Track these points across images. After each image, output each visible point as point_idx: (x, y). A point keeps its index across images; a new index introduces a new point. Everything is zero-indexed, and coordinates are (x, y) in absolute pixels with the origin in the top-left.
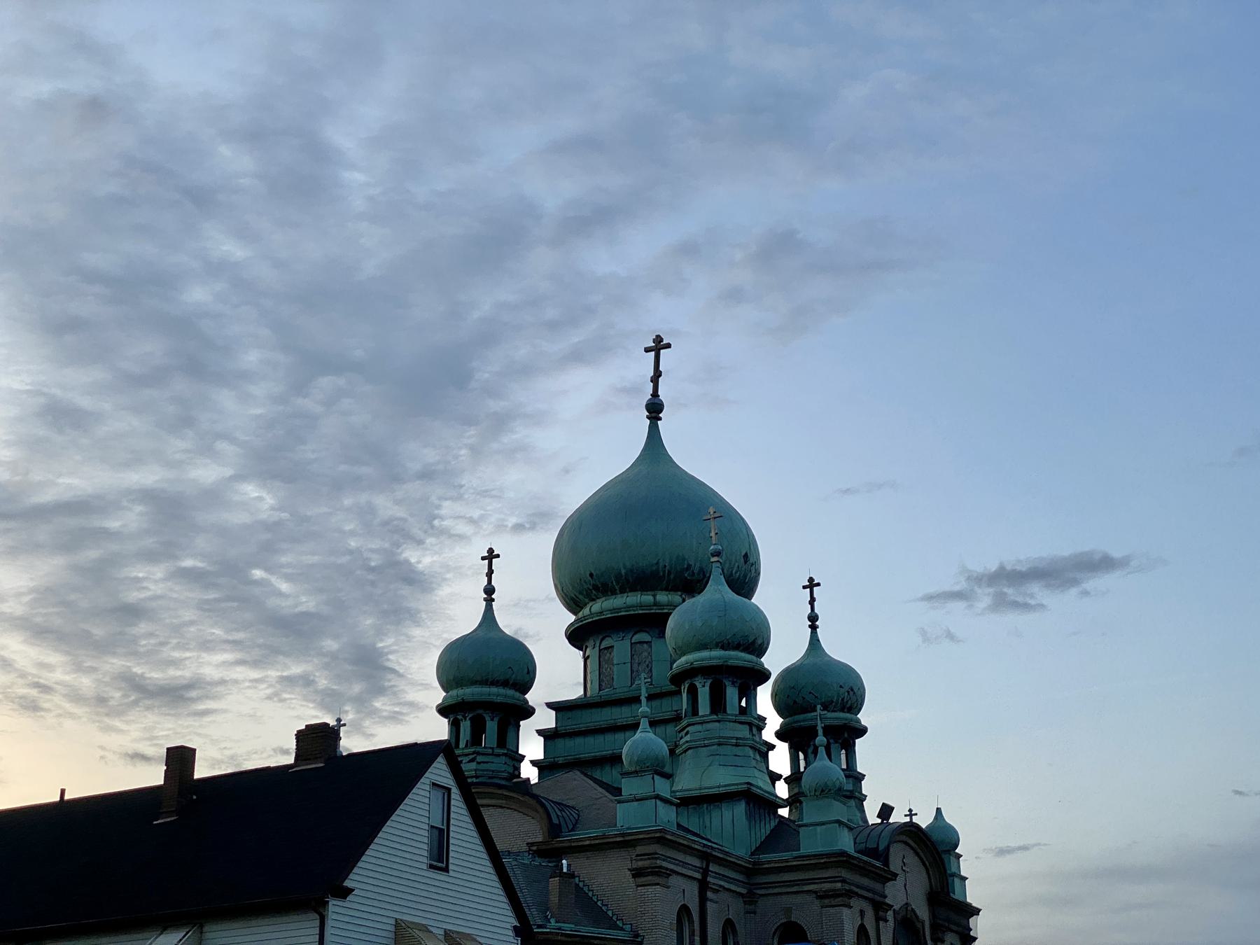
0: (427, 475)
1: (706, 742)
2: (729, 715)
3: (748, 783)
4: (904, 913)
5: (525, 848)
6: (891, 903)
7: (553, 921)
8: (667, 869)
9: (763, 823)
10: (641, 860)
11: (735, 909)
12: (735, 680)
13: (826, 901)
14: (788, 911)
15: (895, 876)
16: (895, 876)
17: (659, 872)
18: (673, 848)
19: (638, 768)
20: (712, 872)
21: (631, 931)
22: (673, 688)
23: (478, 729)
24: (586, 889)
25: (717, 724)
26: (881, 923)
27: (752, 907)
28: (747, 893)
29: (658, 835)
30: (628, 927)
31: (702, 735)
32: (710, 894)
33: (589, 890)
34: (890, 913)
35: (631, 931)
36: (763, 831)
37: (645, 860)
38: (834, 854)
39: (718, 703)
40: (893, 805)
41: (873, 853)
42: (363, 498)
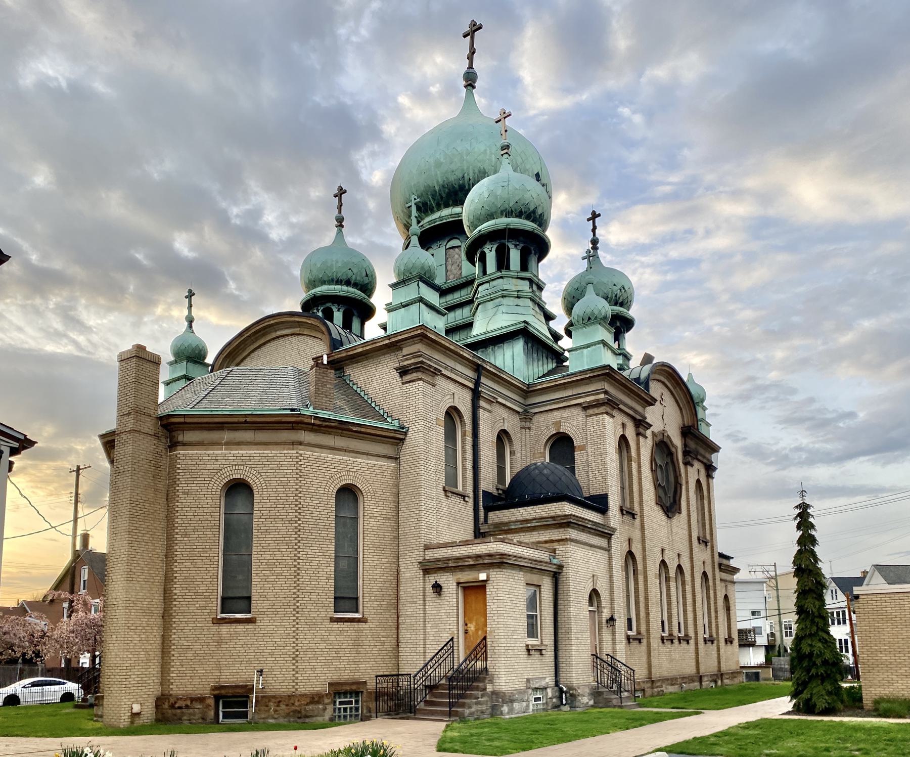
1: (492, 296)
3: (525, 322)
6: (651, 423)
7: (311, 409)
10: (407, 359)
11: (511, 423)
13: (590, 411)
17: (419, 368)
18: (445, 354)
25: (501, 280)
26: (641, 438)
30: (396, 423)
31: (490, 291)
32: (482, 403)
33: (365, 395)
34: (649, 433)
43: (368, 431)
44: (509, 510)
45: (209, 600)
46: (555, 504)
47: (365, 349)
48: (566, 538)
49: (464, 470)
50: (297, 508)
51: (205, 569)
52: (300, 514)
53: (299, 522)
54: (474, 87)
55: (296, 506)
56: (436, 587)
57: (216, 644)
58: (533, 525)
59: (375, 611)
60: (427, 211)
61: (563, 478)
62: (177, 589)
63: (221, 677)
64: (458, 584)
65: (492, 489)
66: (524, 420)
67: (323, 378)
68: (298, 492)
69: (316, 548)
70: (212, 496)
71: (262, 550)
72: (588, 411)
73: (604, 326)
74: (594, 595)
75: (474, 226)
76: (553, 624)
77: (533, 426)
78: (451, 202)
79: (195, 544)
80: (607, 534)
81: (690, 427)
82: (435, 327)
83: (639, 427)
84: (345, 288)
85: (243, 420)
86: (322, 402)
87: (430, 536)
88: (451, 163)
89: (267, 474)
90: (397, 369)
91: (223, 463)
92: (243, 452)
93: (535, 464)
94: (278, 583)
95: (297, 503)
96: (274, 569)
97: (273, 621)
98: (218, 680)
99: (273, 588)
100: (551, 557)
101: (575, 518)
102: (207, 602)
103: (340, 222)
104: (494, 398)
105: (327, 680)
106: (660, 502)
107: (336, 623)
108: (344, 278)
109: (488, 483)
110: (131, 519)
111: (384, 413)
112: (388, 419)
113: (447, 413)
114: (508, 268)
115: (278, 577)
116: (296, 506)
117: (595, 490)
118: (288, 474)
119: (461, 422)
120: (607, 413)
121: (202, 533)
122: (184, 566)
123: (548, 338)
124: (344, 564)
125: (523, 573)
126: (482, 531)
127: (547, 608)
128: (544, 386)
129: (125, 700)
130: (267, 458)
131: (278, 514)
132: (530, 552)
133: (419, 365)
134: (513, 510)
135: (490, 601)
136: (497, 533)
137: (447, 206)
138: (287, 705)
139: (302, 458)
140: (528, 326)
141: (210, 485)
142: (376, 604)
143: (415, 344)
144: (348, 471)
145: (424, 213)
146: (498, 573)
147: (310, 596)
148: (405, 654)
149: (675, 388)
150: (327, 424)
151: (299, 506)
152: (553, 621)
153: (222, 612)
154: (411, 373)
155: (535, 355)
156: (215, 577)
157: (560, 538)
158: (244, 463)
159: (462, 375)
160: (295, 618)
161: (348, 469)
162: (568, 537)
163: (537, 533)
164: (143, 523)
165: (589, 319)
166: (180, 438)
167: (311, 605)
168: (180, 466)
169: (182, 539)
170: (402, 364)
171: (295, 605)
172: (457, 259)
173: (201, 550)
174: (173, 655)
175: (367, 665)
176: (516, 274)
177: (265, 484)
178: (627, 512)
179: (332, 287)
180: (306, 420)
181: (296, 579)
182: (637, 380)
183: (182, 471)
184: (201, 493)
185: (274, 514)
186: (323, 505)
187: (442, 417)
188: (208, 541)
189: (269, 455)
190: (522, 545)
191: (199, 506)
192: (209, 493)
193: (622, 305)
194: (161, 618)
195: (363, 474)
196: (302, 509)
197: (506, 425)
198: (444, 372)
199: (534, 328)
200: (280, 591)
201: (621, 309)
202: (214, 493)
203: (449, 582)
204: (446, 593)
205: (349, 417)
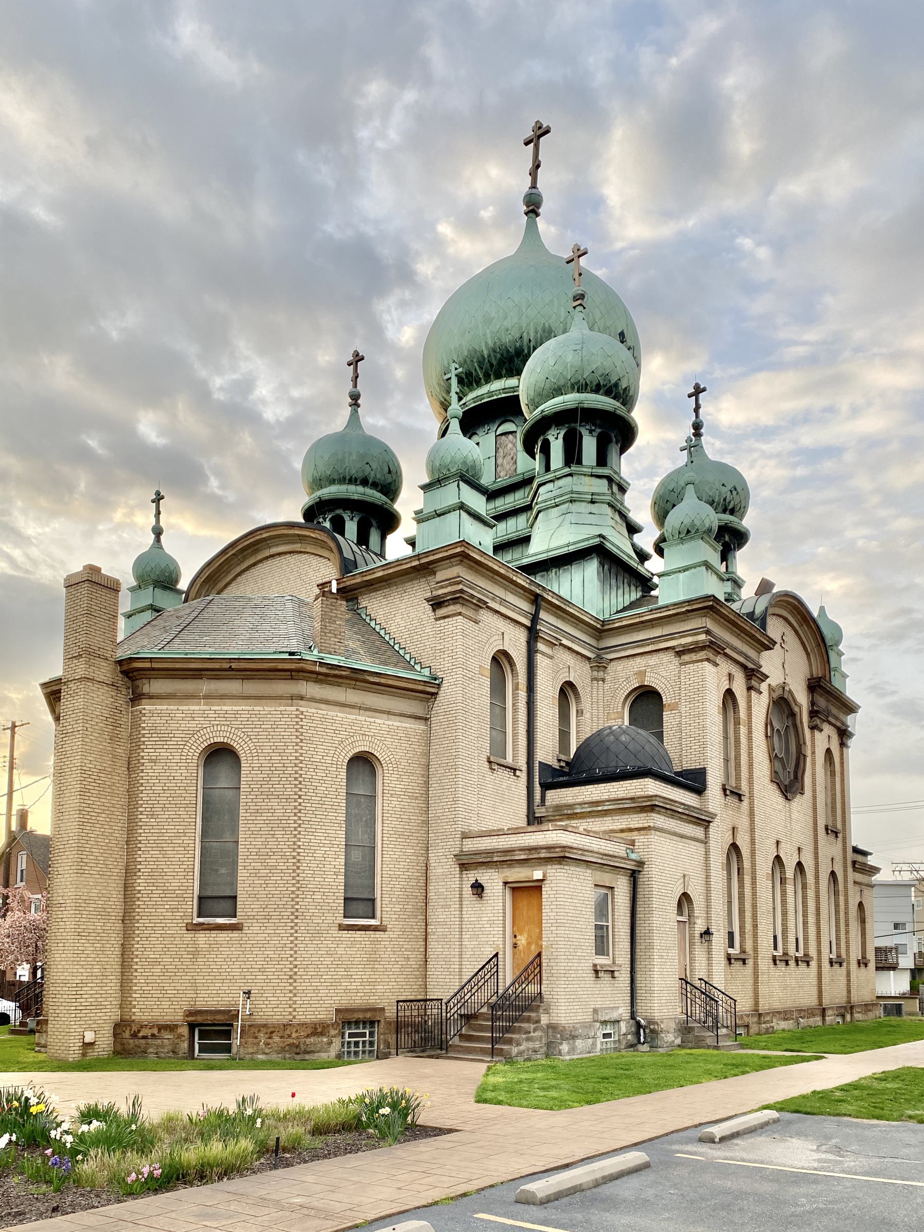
1: (556, 500)
3: (600, 536)
6: (767, 673)
7: (315, 652)
10: (442, 587)
13: (686, 658)
17: (458, 598)
26: (753, 693)
31: (555, 493)
34: (764, 687)
37: (446, 587)
43: (390, 682)
44: (574, 788)
45: (182, 899)
46: (634, 781)
47: (386, 572)
48: (649, 826)
49: (515, 735)
50: (297, 782)
51: (178, 859)
52: (300, 789)
53: (300, 800)
54: (537, 215)
55: (296, 779)
56: (477, 887)
57: (192, 956)
58: (606, 808)
59: (397, 916)
60: (471, 384)
61: (647, 747)
62: (141, 884)
63: (197, 999)
64: (506, 883)
66: (596, 668)
67: (331, 612)
68: (298, 761)
69: (321, 834)
70: (187, 765)
71: (252, 836)
72: (683, 657)
73: (707, 543)
74: (685, 900)
75: (535, 404)
76: (629, 937)
78: (504, 372)
79: (165, 827)
80: (704, 821)
81: (820, 678)
82: (480, 544)
83: (751, 679)
85: (226, 666)
86: (330, 644)
87: (469, 821)
88: (505, 319)
89: (258, 737)
90: (428, 600)
91: (201, 722)
92: (228, 707)
93: (610, 728)
94: (272, 878)
95: (297, 776)
96: (267, 861)
97: (264, 928)
98: (193, 1003)
99: (265, 886)
100: (628, 851)
101: (661, 800)
102: (180, 903)
103: (355, 398)
104: (557, 639)
105: (333, 1005)
107: (346, 932)
109: (547, 752)
110: (82, 793)
111: (410, 659)
113: (494, 659)
114: (579, 462)
115: (272, 871)
116: (296, 779)
117: (689, 764)
118: (285, 737)
119: (512, 671)
120: (708, 660)
121: (174, 813)
122: (150, 856)
123: (631, 558)
124: (356, 855)
125: (590, 871)
126: (537, 815)
127: (622, 918)
128: (625, 623)
129: (74, 1027)
130: (258, 716)
131: (273, 790)
132: (601, 844)
133: (458, 595)
134: (579, 788)
135: (547, 907)
136: (557, 817)
137: (498, 377)
138: (282, 1037)
139: (303, 717)
141: (184, 750)
142: (398, 908)
143: (453, 566)
144: (363, 735)
145: (468, 387)
146: (558, 870)
147: (313, 897)
148: (435, 973)
149: (801, 626)
150: (336, 672)
151: (300, 779)
152: (629, 934)
153: (199, 916)
154: (447, 606)
155: (613, 582)
156: (191, 870)
157: (641, 826)
158: (229, 723)
159: (515, 608)
160: (293, 924)
161: (363, 733)
162: (652, 825)
163: (610, 818)
164: (97, 799)
165: (688, 532)
166: (146, 689)
167: (314, 907)
168: (145, 725)
169: (148, 820)
170: (436, 593)
171: (293, 908)
172: (511, 449)
173: (173, 835)
174: (136, 970)
175: (385, 987)
177: (255, 751)
178: (731, 792)
180: (312, 668)
181: (295, 875)
182: (751, 615)
183: (148, 732)
184: (172, 761)
185: (268, 790)
186: (330, 779)
188: (181, 824)
189: (261, 712)
190: (591, 834)
191: (170, 778)
192: (182, 761)
193: (732, 512)
194: (120, 922)
195: (383, 739)
196: (303, 783)
197: (572, 675)
198: (491, 604)
199: (613, 544)
200: (274, 889)
201: (731, 518)
202: (190, 761)
203: (493, 880)
204: (489, 895)
205: (365, 664)
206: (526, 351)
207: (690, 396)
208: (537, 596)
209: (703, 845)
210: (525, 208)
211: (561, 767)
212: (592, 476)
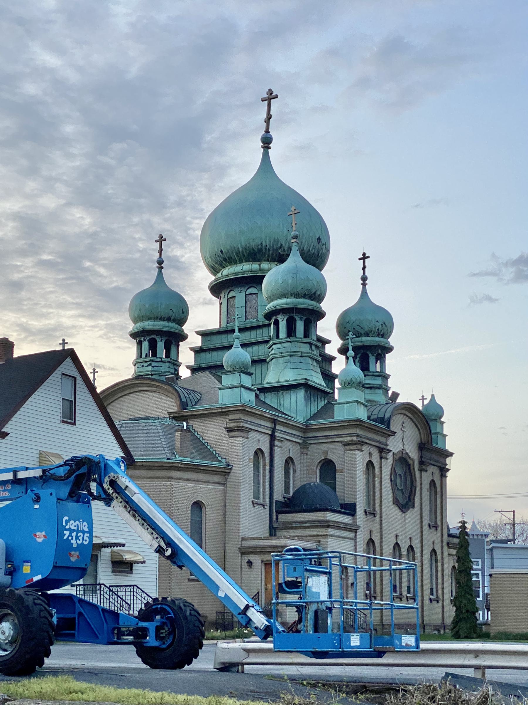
0: (180, 203)
1: (283, 354)
2: (298, 338)
3: (305, 379)
4: (401, 455)
5: (168, 415)
8: (247, 428)
9: (316, 403)
10: (232, 423)
11: (293, 451)
12: (302, 317)
13: (348, 447)
14: (326, 453)
15: (394, 433)
16: (394, 433)
17: (241, 429)
19: (232, 369)
20: (277, 430)
21: (226, 463)
22: (267, 322)
23: (153, 346)
24: (201, 439)
25: (289, 343)
26: (383, 460)
27: (305, 450)
28: (302, 443)
29: (241, 408)
30: (224, 461)
32: (276, 443)
33: (203, 440)
34: (390, 455)
35: (226, 463)
36: (316, 407)
37: (234, 422)
38: (352, 420)
39: (291, 331)
40: (398, 392)
41: (381, 420)
42: (146, 217)
54: (270, 148)
60: (232, 262)
64: (262, 561)
65: (281, 499)
75: (271, 299)
77: (309, 452)
78: (251, 259)
81: (425, 444)
83: (382, 453)
84: (166, 323)
90: (226, 428)
93: (310, 484)
100: (317, 546)
106: (396, 502)
108: (166, 316)
109: (278, 496)
112: (219, 458)
113: (256, 453)
117: (347, 501)
134: (294, 514)
137: (247, 261)
140: (308, 382)
162: (328, 534)
163: (309, 530)
170: (228, 426)
172: (254, 303)
176: (300, 340)
179: (157, 323)
187: (252, 456)
193: (383, 336)
197: (291, 453)
205: (198, 461)
206: (264, 251)
207: (360, 259)
208: (275, 420)
209: (353, 541)
210: (262, 144)
211: (285, 501)
212: (301, 342)
